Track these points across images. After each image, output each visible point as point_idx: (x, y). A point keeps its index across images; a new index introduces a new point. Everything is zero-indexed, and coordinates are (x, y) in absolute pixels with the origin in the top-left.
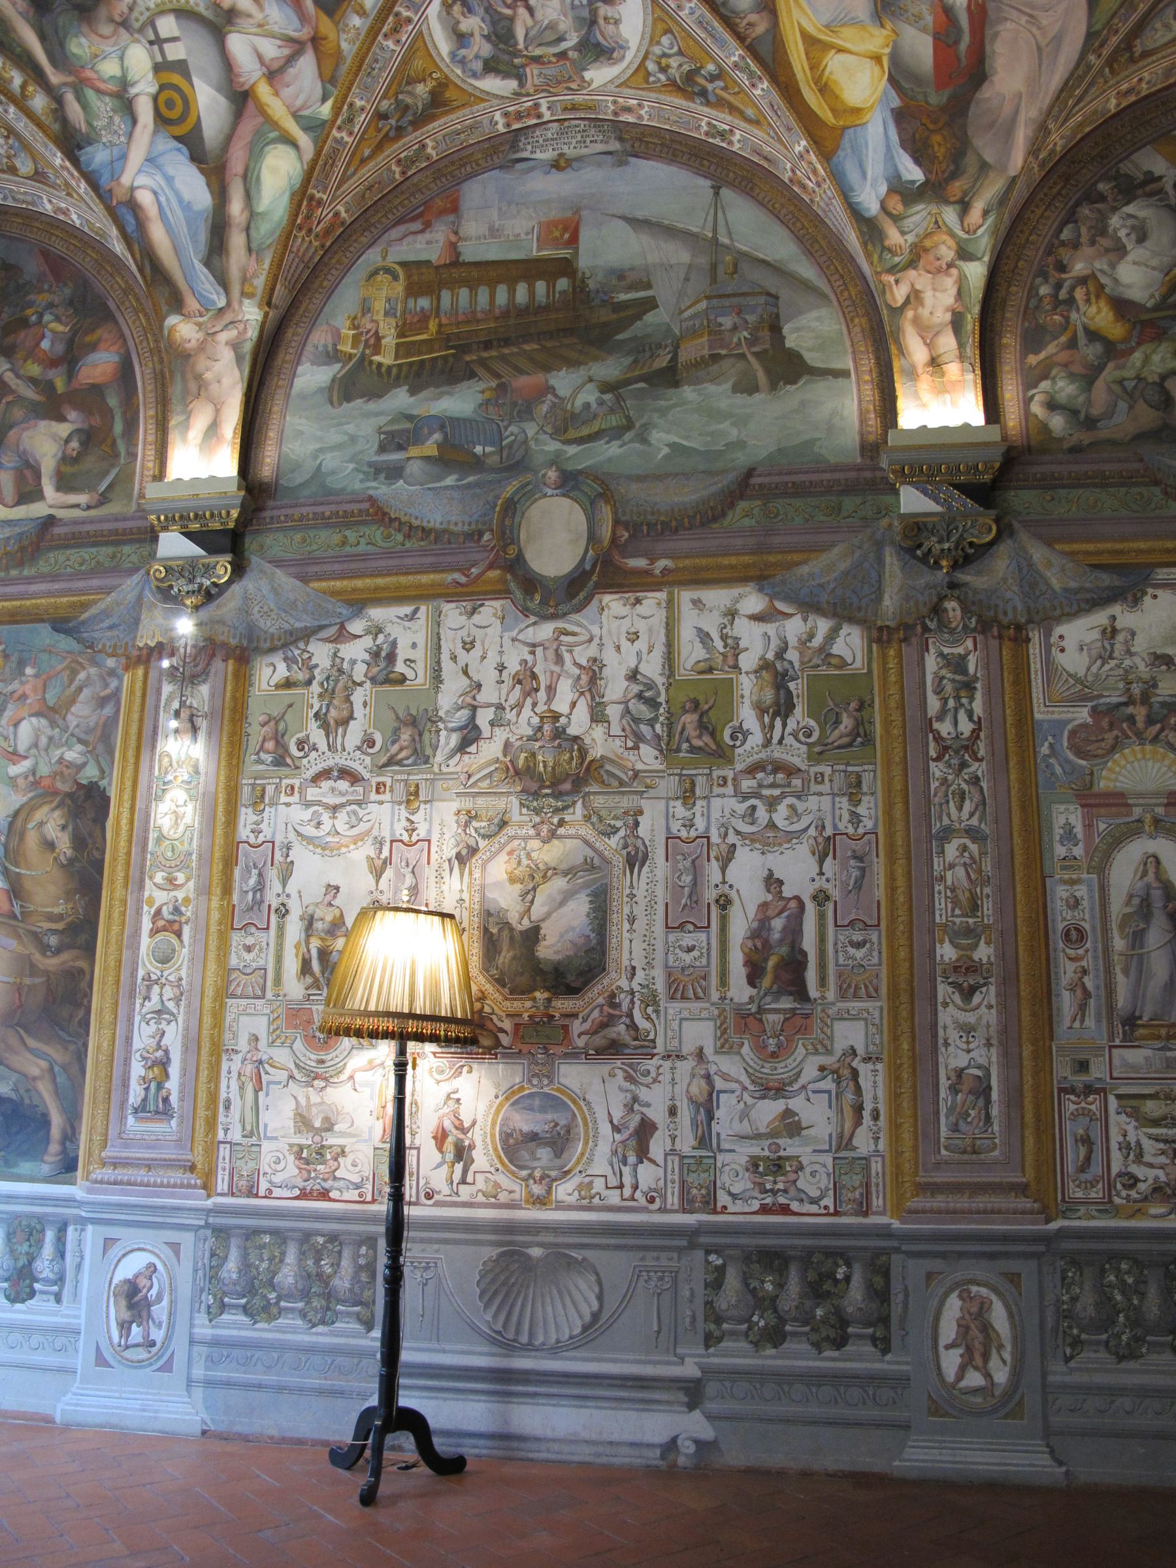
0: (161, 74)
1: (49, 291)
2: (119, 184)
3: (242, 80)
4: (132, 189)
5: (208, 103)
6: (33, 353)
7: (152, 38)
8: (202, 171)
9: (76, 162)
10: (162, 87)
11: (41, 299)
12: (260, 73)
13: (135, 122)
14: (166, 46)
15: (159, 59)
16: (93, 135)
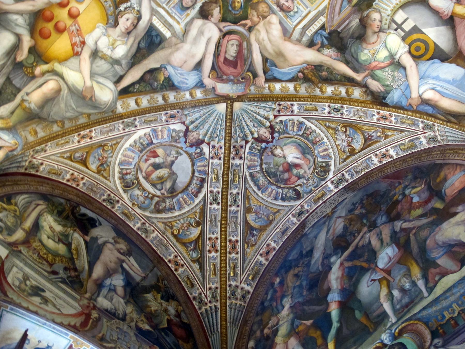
0: (407, 40)
1: (400, 184)
2: (412, 99)
3: (446, 13)
4: (420, 96)
5: (437, 35)
6: (412, 207)
7: (395, 27)
8: (451, 62)
9: (386, 105)
10: (410, 45)
11: (399, 189)
12: (453, 4)
13: (405, 69)
14: (403, 26)
15: (403, 34)
16: (388, 88)
